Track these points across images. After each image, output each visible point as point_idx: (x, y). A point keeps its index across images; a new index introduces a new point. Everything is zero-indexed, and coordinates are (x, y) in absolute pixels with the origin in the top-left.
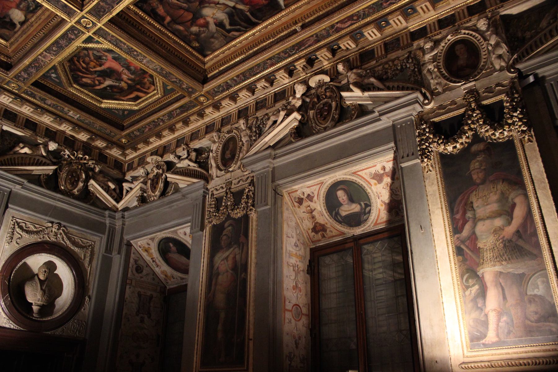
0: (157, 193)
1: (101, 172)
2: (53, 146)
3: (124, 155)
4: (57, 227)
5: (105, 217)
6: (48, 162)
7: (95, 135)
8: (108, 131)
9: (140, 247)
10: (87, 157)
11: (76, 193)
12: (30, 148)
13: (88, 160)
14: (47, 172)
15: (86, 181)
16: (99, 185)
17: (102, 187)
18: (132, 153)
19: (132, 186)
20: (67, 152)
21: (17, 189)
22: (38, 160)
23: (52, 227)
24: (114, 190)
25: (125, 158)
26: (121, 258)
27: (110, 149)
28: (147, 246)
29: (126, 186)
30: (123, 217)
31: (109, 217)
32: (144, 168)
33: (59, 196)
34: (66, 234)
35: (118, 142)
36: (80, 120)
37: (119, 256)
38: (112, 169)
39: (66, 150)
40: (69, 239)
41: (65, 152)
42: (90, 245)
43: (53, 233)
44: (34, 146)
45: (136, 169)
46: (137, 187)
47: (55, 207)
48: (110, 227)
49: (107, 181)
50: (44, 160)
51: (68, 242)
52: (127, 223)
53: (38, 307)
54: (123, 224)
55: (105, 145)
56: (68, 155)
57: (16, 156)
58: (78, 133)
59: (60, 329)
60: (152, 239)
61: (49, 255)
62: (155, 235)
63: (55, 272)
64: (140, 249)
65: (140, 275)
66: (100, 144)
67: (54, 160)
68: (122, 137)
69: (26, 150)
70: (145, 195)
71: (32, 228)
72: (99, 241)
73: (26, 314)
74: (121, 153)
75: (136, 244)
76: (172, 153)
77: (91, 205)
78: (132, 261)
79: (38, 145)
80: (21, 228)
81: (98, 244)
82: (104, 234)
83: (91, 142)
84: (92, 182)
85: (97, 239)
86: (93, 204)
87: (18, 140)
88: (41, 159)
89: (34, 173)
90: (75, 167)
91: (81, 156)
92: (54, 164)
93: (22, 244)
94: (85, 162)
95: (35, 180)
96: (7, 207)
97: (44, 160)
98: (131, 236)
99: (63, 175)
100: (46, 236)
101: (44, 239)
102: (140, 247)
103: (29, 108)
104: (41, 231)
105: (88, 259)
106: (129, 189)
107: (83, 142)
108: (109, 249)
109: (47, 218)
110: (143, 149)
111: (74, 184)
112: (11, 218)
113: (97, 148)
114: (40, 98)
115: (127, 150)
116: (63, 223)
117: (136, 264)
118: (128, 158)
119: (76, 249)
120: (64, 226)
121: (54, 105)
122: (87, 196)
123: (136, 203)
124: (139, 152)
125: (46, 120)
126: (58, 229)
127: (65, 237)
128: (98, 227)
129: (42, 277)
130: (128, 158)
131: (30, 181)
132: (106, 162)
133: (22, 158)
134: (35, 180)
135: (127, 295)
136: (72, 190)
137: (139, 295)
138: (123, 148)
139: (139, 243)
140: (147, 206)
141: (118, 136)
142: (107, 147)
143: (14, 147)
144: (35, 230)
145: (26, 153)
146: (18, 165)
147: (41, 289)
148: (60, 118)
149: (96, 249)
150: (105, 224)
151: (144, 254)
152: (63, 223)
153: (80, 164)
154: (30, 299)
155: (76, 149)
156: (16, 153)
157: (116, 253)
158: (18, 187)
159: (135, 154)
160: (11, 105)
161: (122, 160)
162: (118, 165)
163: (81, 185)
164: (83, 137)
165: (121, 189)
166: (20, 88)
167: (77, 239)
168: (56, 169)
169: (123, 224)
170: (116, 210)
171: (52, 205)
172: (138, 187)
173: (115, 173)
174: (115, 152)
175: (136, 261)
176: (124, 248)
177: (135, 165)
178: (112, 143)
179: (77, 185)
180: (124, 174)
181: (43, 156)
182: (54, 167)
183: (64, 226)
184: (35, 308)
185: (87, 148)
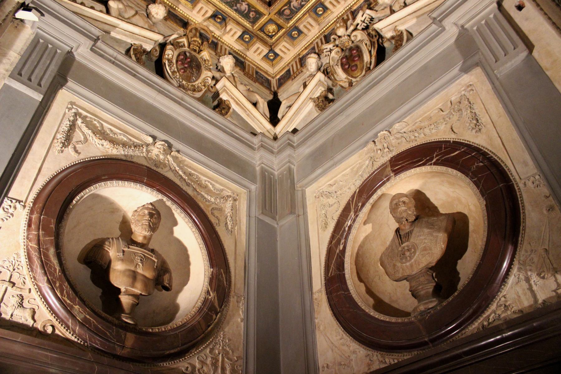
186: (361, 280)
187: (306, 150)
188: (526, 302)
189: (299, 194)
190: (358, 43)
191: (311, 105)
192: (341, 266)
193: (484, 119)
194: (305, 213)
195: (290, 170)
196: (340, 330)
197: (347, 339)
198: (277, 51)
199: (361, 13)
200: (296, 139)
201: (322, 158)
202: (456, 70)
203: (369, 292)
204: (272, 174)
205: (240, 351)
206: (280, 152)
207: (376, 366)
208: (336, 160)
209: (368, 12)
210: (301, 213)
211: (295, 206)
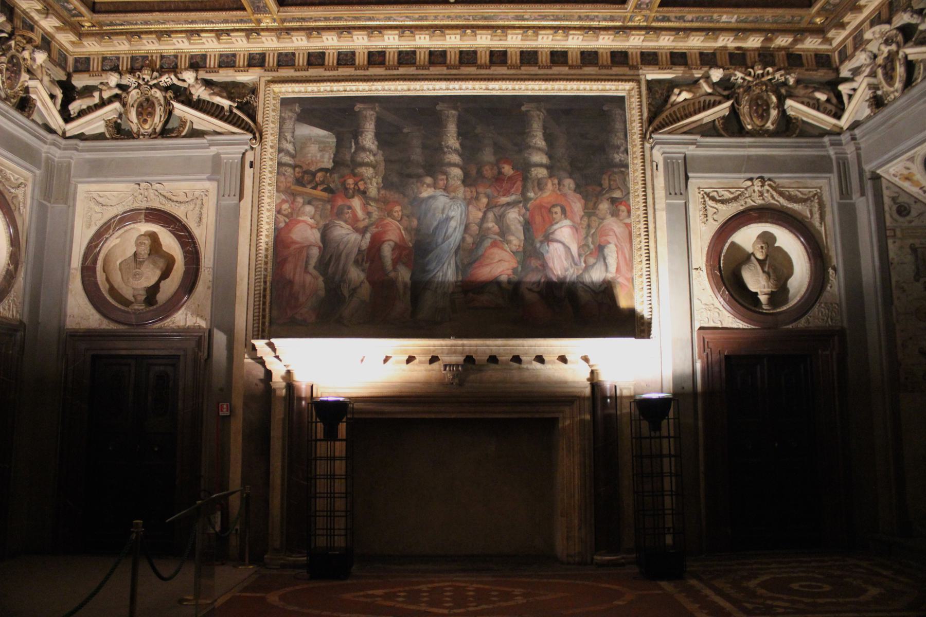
0: (898, 85)
1: (798, 82)
2: (716, 75)
3: (828, 41)
4: (760, 184)
5: (824, 147)
6: (718, 98)
7: (770, 32)
8: (788, 18)
9: (895, 175)
10: (770, 69)
11: (772, 127)
12: (689, 91)
13: (773, 73)
14: (721, 114)
15: (780, 105)
16: (803, 103)
17: (808, 105)
18: (838, 34)
19: (854, 85)
20: (739, 75)
21: (691, 150)
22: (705, 101)
23: (753, 185)
24: (828, 101)
25: (831, 44)
26: (867, 200)
27: (802, 41)
28: (906, 172)
29: (844, 88)
30: (854, 138)
31: (832, 144)
32: (864, 50)
33: (748, 140)
34: (774, 189)
35: (810, 26)
36: (742, 21)
37: (864, 198)
38: (813, 70)
39: (737, 73)
40: (781, 194)
41: (735, 75)
42: (815, 195)
43: (757, 194)
44: (693, 84)
45: (853, 56)
46: (862, 85)
47: (749, 157)
48: (837, 159)
49: (813, 92)
50: (712, 98)
51: (781, 200)
52: (862, 146)
53: (767, 296)
54: (858, 149)
55: (790, 40)
56: (742, 78)
57: (675, 108)
58: (745, 39)
59: (803, 320)
60: (911, 159)
61: (760, 225)
62: (913, 152)
63: (776, 245)
64: (897, 179)
65: (908, 218)
66: (783, 41)
67: (726, 93)
68: (814, 17)
69: (685, 95)
70: (879, 93)
71: (727, 195)
72: (826, 185)
73: (753, 308)
74: (820, 40)
75: (887, 172)
76: (905, 11)
77: (799, 136)
78: (887, 200)
79: (696, 82)
80: (713, 199)
81: (826, 189)
82: (831, 171)
83: (769, 45)
84: (789, 103)
85: (823, 182)
86: (802, 135)
87: (671, 85)
88: (708, 98)
89: (705, 121)
90: (758, 91)
91: (760, 72)
92: (727, 98)
93: (722, 219)
94: (770, 77)
95: (709, 130)
96: (687, 178)
97: (712, 98)
98: (875, 164)
99: (744, 109)
100: (749, 200)
101: (748, 205)
102: (895, 175)
103: (667, 38)
104: (740, 195)
105: (817, 216)
106: (851, 92)
107: (757, 49)
108: (845, 192)
109: (742, 175)
110: (853, 20)
111: (764, 116)
112: (697, 190)
113: (780, 49)
114: (676, 17)
115: (829, 31)
116: (766, 176)
117: (895, 203)
118: (835, 43)
119: (796, 207)
120: (769, 179)
121: (697, 18)
122: (788, 126)
123: (867, 112)
124: (849, 28)
125: (696, 42)
126: (762, 186)
127: (775, 194)
128: (819, 166)
129: (760, 256)
130: (835, 43)
131: (703, 135)
132: (801, 65)
133: (683, 107)
134: (709, 130)
135: (892, 255)
136: (763, 126)
137: (914, 249)
138: (820, 31)
139: (892, 171)
140: (886, 112)
141: (807, 19)
142: (795, 41)
143: (669, 97)
144: (732, 196)
145: (685, 100)
146: (683, 119)
147: (764, 272)
148: (713, 31)
149: (826, 198)
150: (829, 157)
151: (906, 185)
152: (766, 176)
153: (765, 84)
154: (753, 288)
155: (749, 64)
156: (672, 105)
157: (859, 194)
158: (692, 147)
159: (844, 34)
160: (645, 44)
161: (828, 50)
162: (822, 60)
163: (774, 113)
164: (754, 42)
165: (839, 96)
166: (646, 18)
167: (793, 192)
168: (733, 104)
169: (858, 149)
170: (839, 132)
171: (744, 156)
172: (864, 85)
173: (821, 75)
174: (811, 44)
175: (894, 199)
176: (869, 185)
177: (850, 51)
178: (800, 32)
179: (769, 115)
180: (837, 70)
181: (710, 94)
182: (729, 103)
183: (769, 179)
184: (763, 298)
185: (766, 57)
186: (104, 271)
187: (88, 156)
188: (182, 324)
189: (72, 188)
190: (155, 101)
191: (102, 123)
192: (95, 261)
193: (204, 220)
194: (74, 205)
195: (69, 164)
196: (86, 300)
197: (90, 307)
198: (85, 43)
199: (167, 76)
200: (82, 144)
201: (97, 170)
202: (204, 177)
203: (108, 280)
204: (53, 161)
205: (20, 300)
206: (65, 149)
207: (104, 327)
208: (109, 179)
209: (173, 77)
210: (71, 204)
211: (67, 197)
